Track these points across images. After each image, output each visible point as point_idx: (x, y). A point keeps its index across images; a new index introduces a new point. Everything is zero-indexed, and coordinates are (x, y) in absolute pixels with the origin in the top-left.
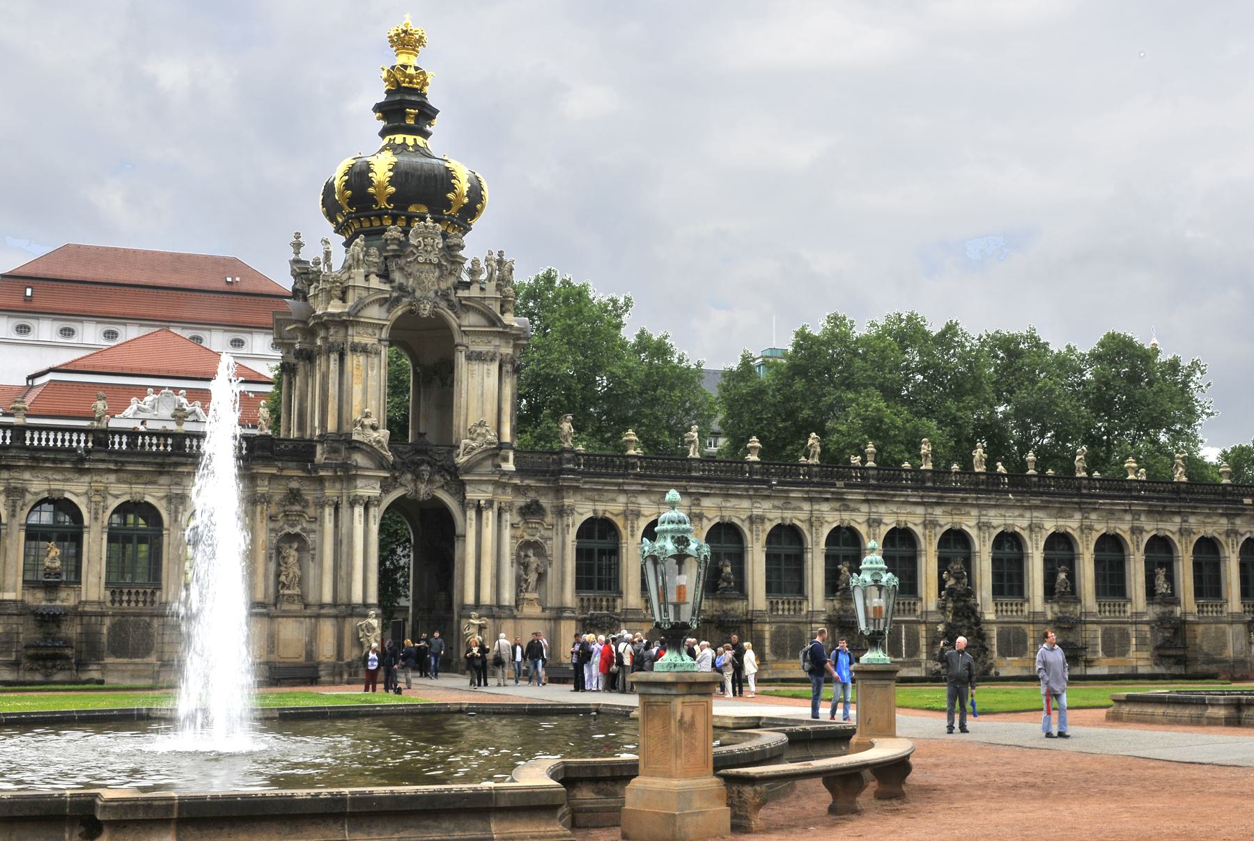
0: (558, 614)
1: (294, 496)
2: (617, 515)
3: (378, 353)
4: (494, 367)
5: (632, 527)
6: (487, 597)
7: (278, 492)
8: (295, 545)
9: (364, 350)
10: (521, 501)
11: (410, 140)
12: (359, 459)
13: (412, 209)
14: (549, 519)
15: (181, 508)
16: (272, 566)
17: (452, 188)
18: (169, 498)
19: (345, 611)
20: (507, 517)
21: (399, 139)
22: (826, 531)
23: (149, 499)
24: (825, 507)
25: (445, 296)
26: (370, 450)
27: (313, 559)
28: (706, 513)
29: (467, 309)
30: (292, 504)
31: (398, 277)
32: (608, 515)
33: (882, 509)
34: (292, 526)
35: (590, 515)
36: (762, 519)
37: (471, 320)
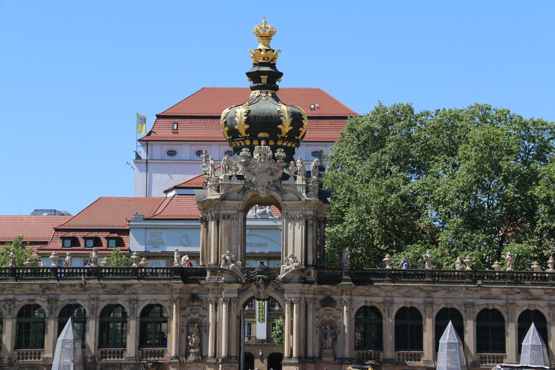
2: (379, 304)
3: (237, 219)
5: (388, 311)
7: (187, 296)
8: (196, 325)
13: (261, 135)
15: (136, 306)
16: (184, 335)
17: (281, 122)
18: (130, 301)
20: (310, 306)
23: (119, 302)
27: (205, 332)
28: (435, 301)
30: (193, 301)
32: (374, 304)
34: (194, 313)
35: (363, 304)
36: (473, 305)
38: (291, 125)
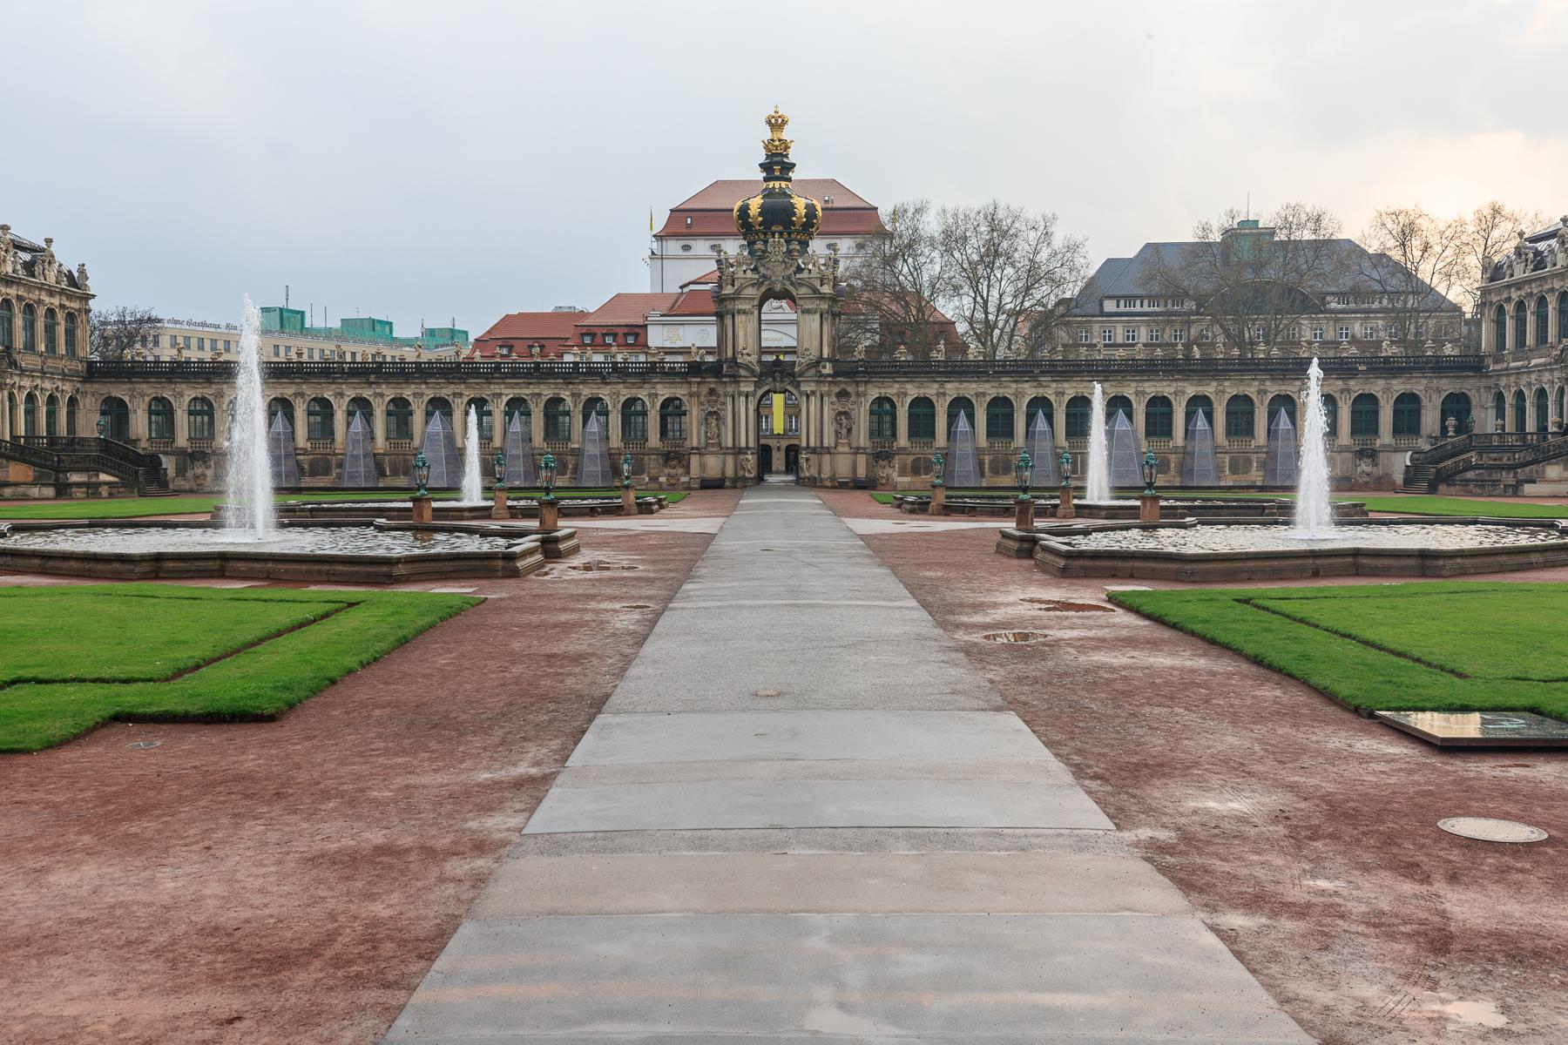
0: (857, 451)
1: (712, 392)
4: (817, 316)
6: (812, 444)
7: (704, 390)
9: (744, 312)
10: (837, 389)
11: (777, 184)
12: (742, 372)
14: (853, 398)
16: (703, 429)
17: (794, 214)
19: (738, 451)
21: (771, 185)
22: (1027, 400)
24: (1026, 385)
25: (789, 278)
26: (747, 367)
29: (801, 285)
31: (762, 270)
33: (1066, 385)
36: (984, 394)
37: (803, 291)
38: (806, 215)
